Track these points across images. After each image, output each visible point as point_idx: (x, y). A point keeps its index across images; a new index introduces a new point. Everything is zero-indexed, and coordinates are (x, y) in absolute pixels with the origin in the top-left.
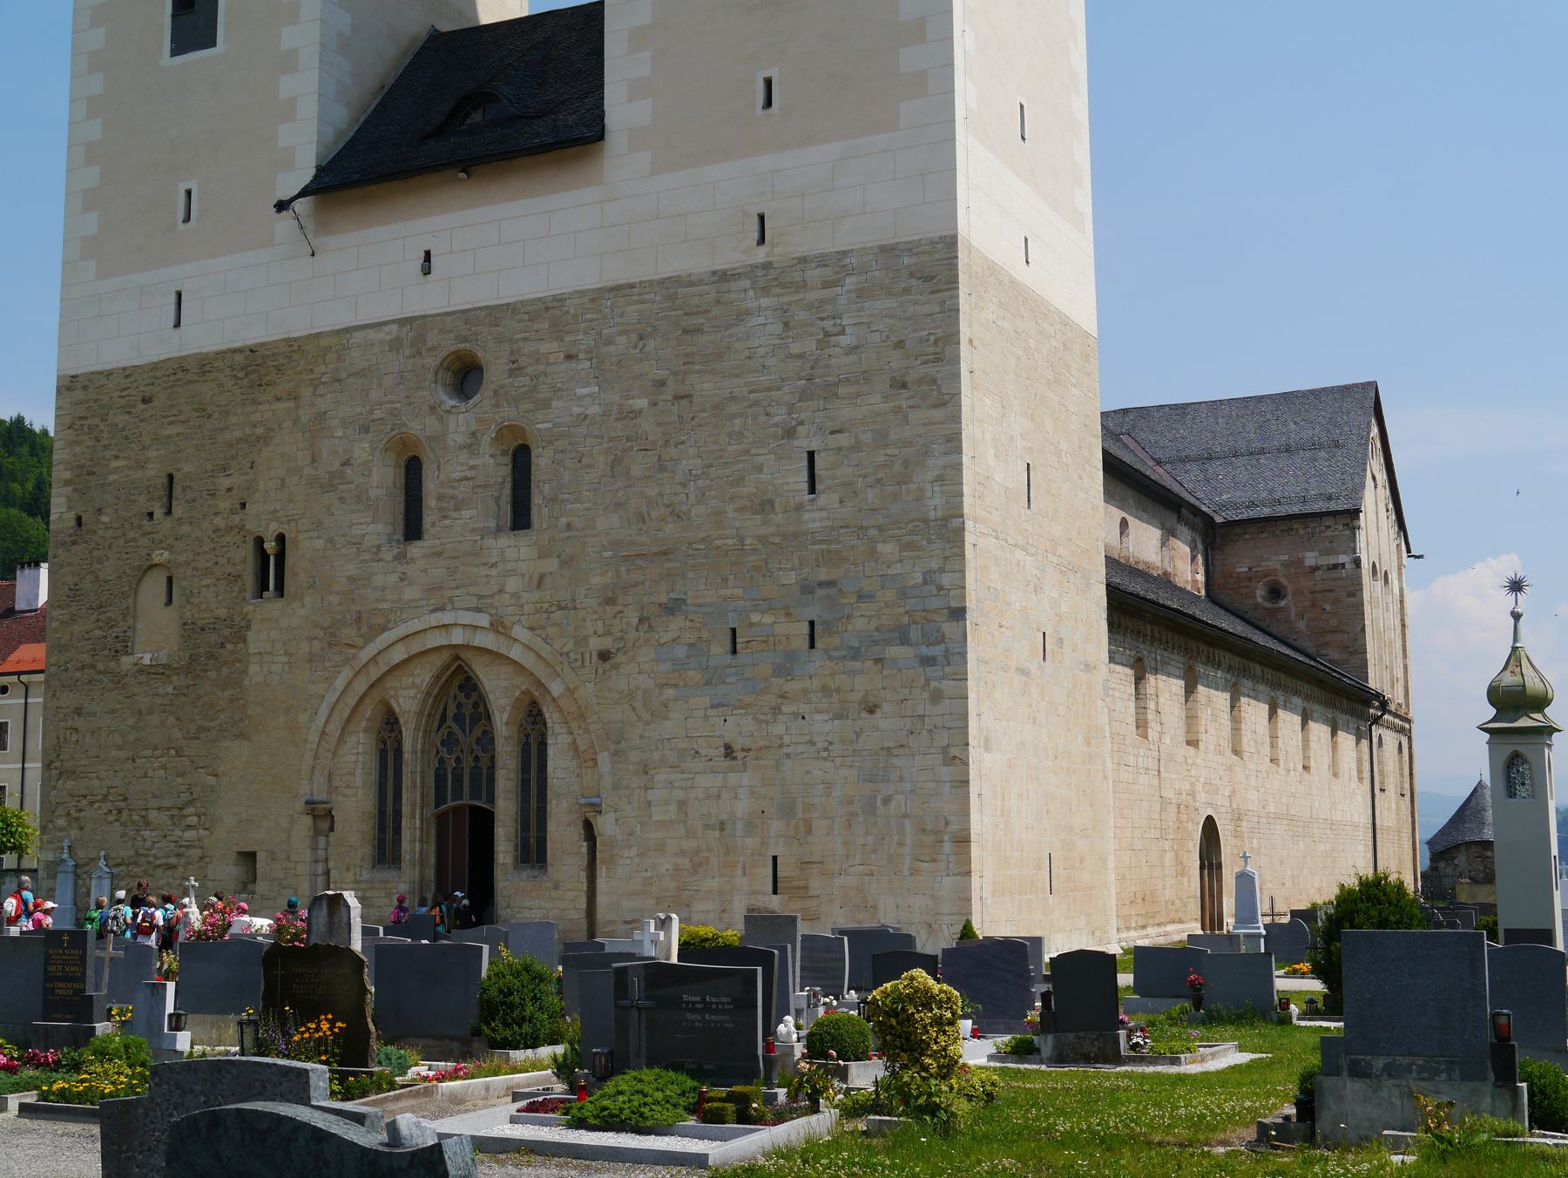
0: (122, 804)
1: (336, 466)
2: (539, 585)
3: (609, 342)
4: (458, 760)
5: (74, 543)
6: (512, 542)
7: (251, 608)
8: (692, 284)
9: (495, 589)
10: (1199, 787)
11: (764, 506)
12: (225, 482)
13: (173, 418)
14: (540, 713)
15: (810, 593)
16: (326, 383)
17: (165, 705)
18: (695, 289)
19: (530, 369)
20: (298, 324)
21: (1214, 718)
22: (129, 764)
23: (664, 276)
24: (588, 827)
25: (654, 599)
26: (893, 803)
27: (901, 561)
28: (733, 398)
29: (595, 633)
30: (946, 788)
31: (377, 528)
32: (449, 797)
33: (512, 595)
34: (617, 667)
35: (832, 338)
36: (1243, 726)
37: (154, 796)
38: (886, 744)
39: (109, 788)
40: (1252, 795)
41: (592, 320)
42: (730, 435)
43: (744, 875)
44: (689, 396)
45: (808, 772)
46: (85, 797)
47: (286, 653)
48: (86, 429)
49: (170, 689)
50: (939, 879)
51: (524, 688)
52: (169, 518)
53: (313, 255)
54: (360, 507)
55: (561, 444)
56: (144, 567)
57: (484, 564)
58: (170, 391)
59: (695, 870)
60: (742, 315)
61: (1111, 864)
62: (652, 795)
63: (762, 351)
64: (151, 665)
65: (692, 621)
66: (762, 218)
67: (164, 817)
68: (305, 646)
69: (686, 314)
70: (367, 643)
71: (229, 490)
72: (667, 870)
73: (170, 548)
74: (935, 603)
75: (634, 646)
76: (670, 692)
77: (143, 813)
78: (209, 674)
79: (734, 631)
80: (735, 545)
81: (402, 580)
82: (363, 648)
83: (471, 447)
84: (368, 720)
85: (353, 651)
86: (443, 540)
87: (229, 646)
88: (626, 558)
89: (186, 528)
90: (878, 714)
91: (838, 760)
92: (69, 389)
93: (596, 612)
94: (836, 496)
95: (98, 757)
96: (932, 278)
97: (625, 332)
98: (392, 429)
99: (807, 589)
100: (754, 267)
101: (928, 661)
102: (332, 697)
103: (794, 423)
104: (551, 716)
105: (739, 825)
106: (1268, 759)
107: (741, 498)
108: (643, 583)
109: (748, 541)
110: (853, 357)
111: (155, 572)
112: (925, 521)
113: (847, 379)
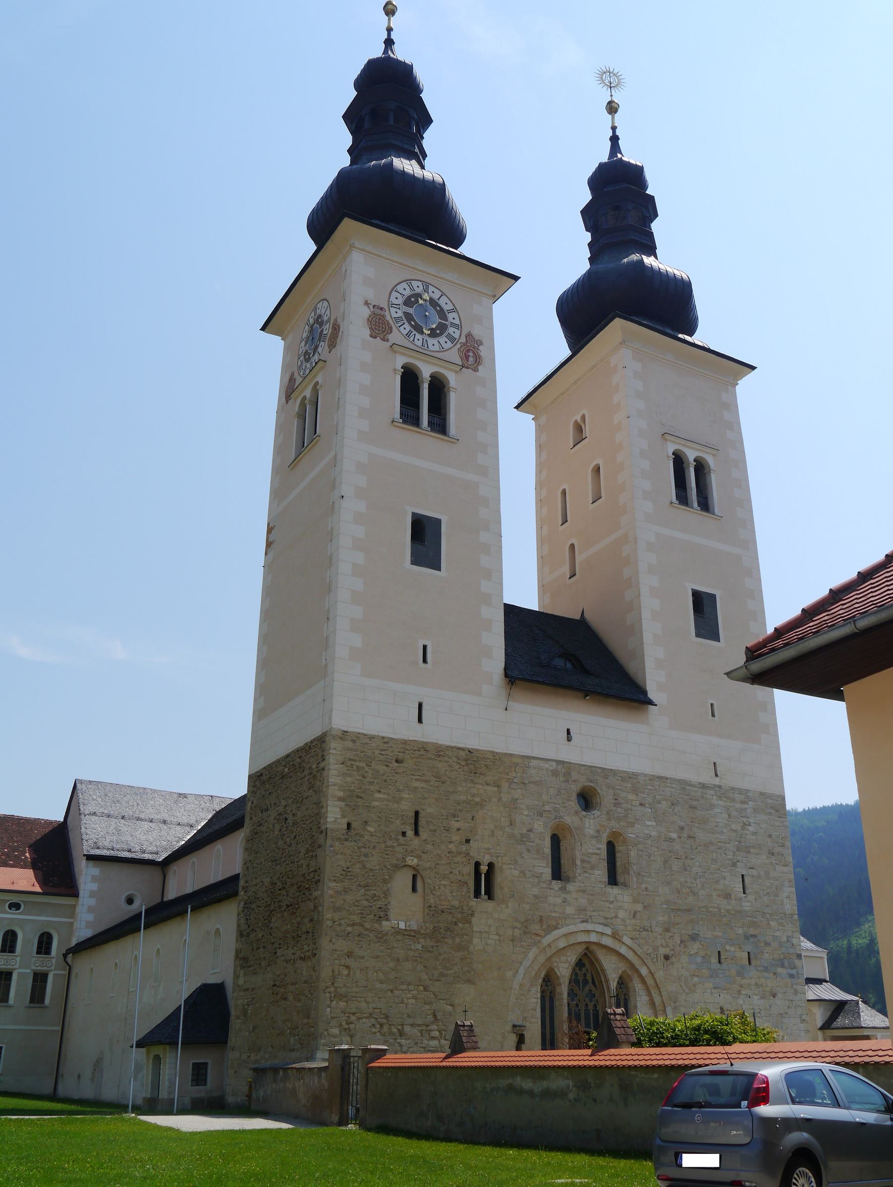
0: (385, 1021)
1: (524, 831)
2: (634, 916)
3: (659, 803)
5: (346, 840)
6: (620, 892)
9: (613, 915)
11: (728, 896)
13: (418, 777)
15: (748, 939)
16: (514, 782)
18: (692, 788)
19: (623, 805)
22: (389, 994)
23: (680, 778)
28: (712, 843)
29: (662, 945)
30: (803, 1034)
34: (672, 964)
35: (747, 826)
37: (409, 1016)
38: (780, 1012)
39: (374, 1008)
42: (712, 860)
44: (694, 838)
46: (354, 1014)
47: (497, 934)
48: (355, 767)
49: (419, 947)
51: (623, 969)
53: (506, 710)
54: (539, 857)
55: (640, 847)
57: (607, 901)
58: (416, 760)
60: (712, 806)
64: (406, 930)
65: (702, 945)
67: (415, 1031)
68: (510, 932)
69: (690, 799)
70: (546, 935)
71: (458, 830)
73: (419, 857)
74: (792, 951)
75: (679, 954)
76: (696, 979)
77: (400, 1027)
79: (719, 952)
80: (717, 912)
82: (544, 937)
85: (539, 938)
86: (586, 884)
87: (460, 925)
88: (673, 910)
89: (429, 847)
90: (776, 998)
92: (341, 738)
93: (661, 934)
94: (753, 897)
95: (366, 987)
96: (778, 811)
97: (665, 800)
98: (555, 818)
99: (747, 937)
101: (791, 976)
102: (527, 963)
103: (735, 861)
104: (637, 985)
107: (719, 890)
109: (722, 911)
110: (754, 837)
111: (405, 870)
112: (785, 914)
113: (753, 846)
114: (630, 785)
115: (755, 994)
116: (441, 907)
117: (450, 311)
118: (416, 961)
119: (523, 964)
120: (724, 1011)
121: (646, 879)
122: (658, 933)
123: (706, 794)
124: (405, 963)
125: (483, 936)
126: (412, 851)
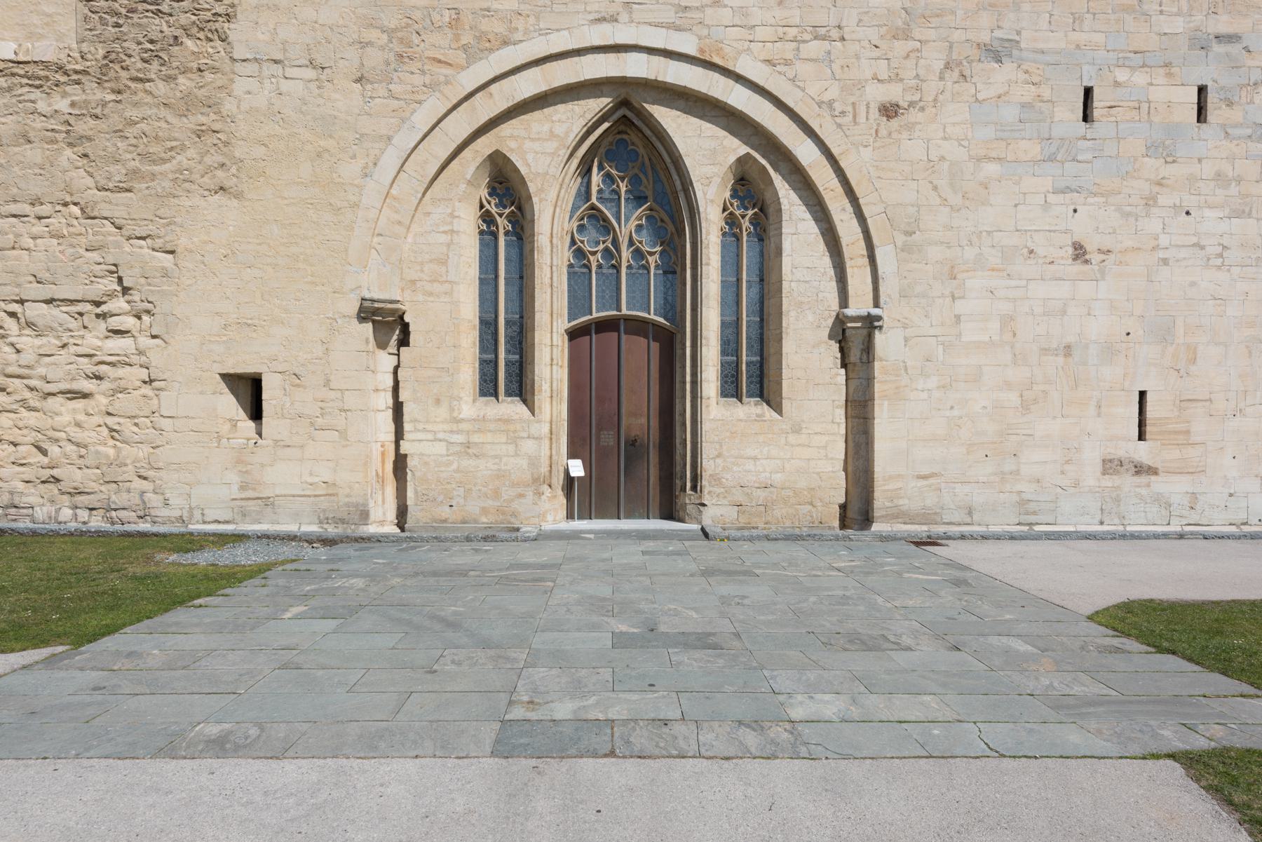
25: (971, 35)
34: (910, 127)
43: (1099, 415)
45: (1193, 284)
49: (63, 105)
59: (1025, 407)
62: (961, 307)
65: (1026, 72)
68: (352, 54)
72: (985, 407)
75: (935, 100)
76: (992, 169)
79: (1088, 92)
82: (463, 68)
99: (1201, 44)
108: (953, 13)
119: (394, 141)
120: (1085, 253)
122: (865, 43)
124: (17, 149)
125: (266, 72)
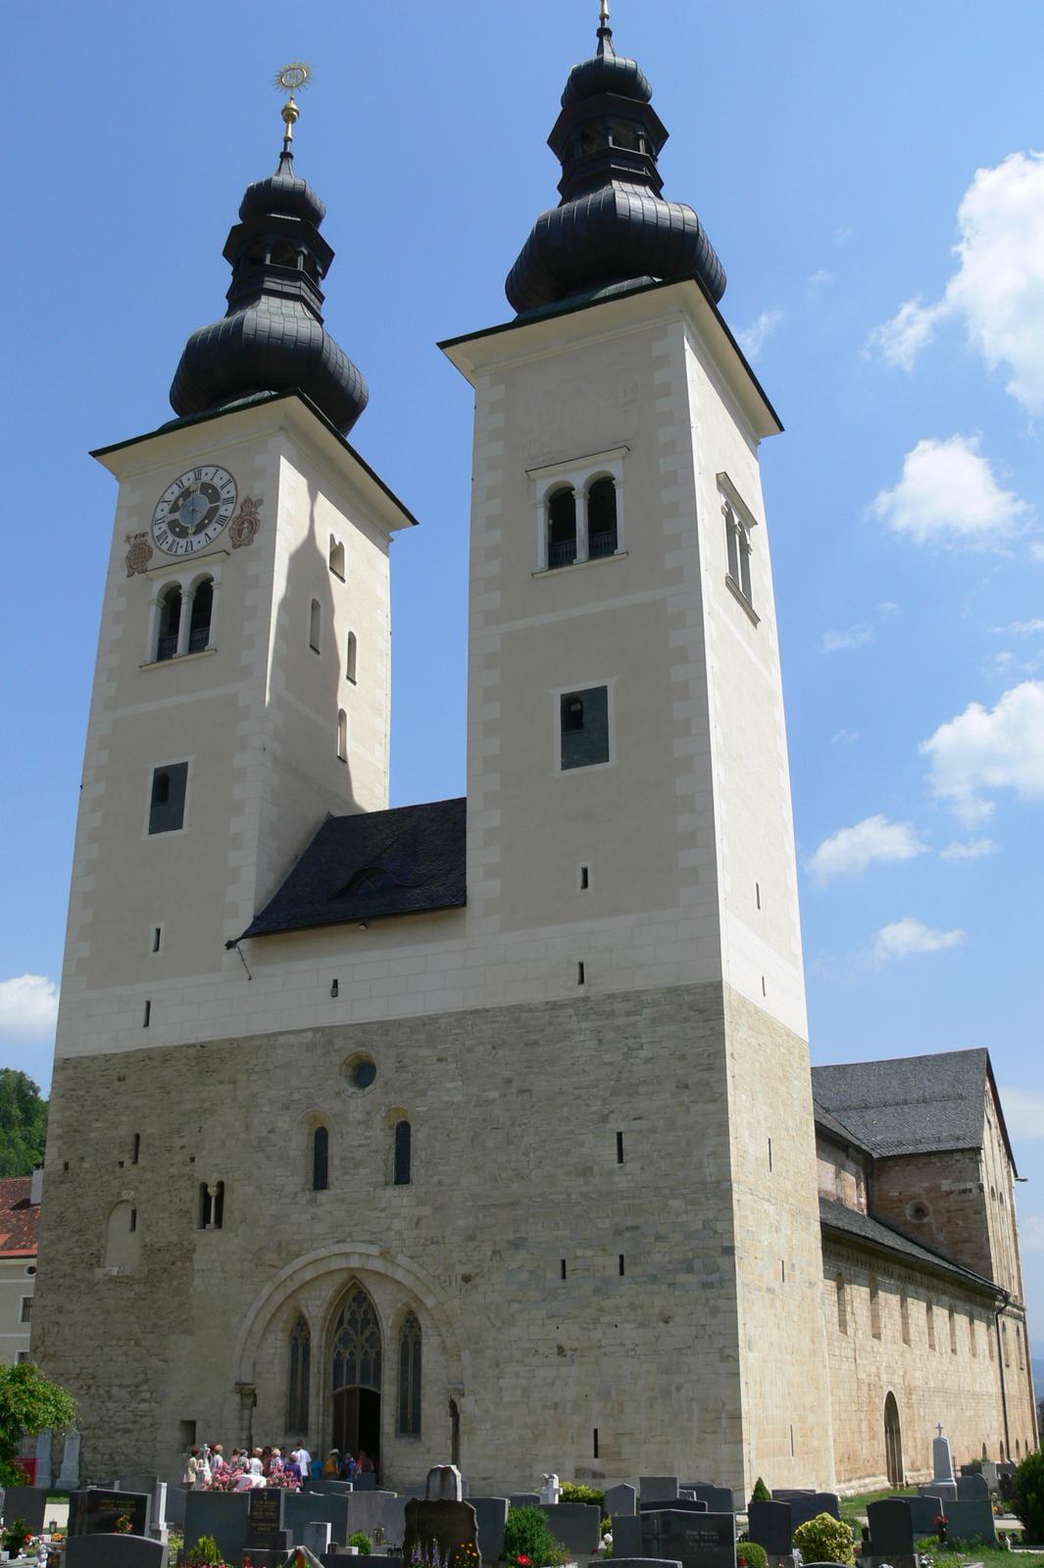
0: (91, 1382)
3: (470, 1050)
4: (351, 1354)
5: (62, 1182)
7: (196, 1236)
8: (530, 1010)
10: (882, 1370)
11: (586, 1172)
12: (179, 1142)
14: (416, 1319)
15: (620, 1234)
16: (257, 1072)
17: (128, 1307)
18: (531, 1014)
20: (239, 1031)
21: (891, 1316)
22: (98, 1351)
24: (453, 1405)
26: (683, 1390)
27: (686, 1212)
31: (295, 1179)
32: (345, 1382)
33: (397, 1232)
34: (476, 1287)
36: (910, 1321)
37: (117, 1376)
40: (918, 1374)
41: (457, 1034)
43: (573, 1443)
44: (529, 1091)
45: (620, 1367)
47: (223, 1270)
48: (74, 1097)
50: (719, 1446)
51: (404, 1300)
52: (136, 1166)
53: (250, 979)
56: (116, 1202)
57: (376, 1209)
61: (831, 1433)
63: (583, 1060)
64: (118, 1277)
66: (581, 966)
67: (124, 1393)
71: (182, 1147)
73: (135, 1189)
76: (516, 1306)
77: (106, 1388)
78: (163, 1284)
79: (564, 1262)
81: (313, 1218)
82: (282, 1268)
83: (367, 1123)
84: (285, 1322)
85: (275, 1270)
87: (179, 1264)
91: (643, 1358)
92: (63, 1068)
97: (482, 1043)
98: (307, 1108)
99: (618, 1232)
100: (576, 1000)
102: (257, 1305)
103: (606, 1112)
104: (424, 1322)
105: (569, 1406)
106: (927, 1346)
109: (574, 1196)
111: (123, 1206)
114: (423, 1036)
115: (628, 1322)
116: (157, 1246)
117: (222, 487)
118: (127, 1311)
121: (440, 1168)
123: (558, 1017)
126: (128, 1183)
